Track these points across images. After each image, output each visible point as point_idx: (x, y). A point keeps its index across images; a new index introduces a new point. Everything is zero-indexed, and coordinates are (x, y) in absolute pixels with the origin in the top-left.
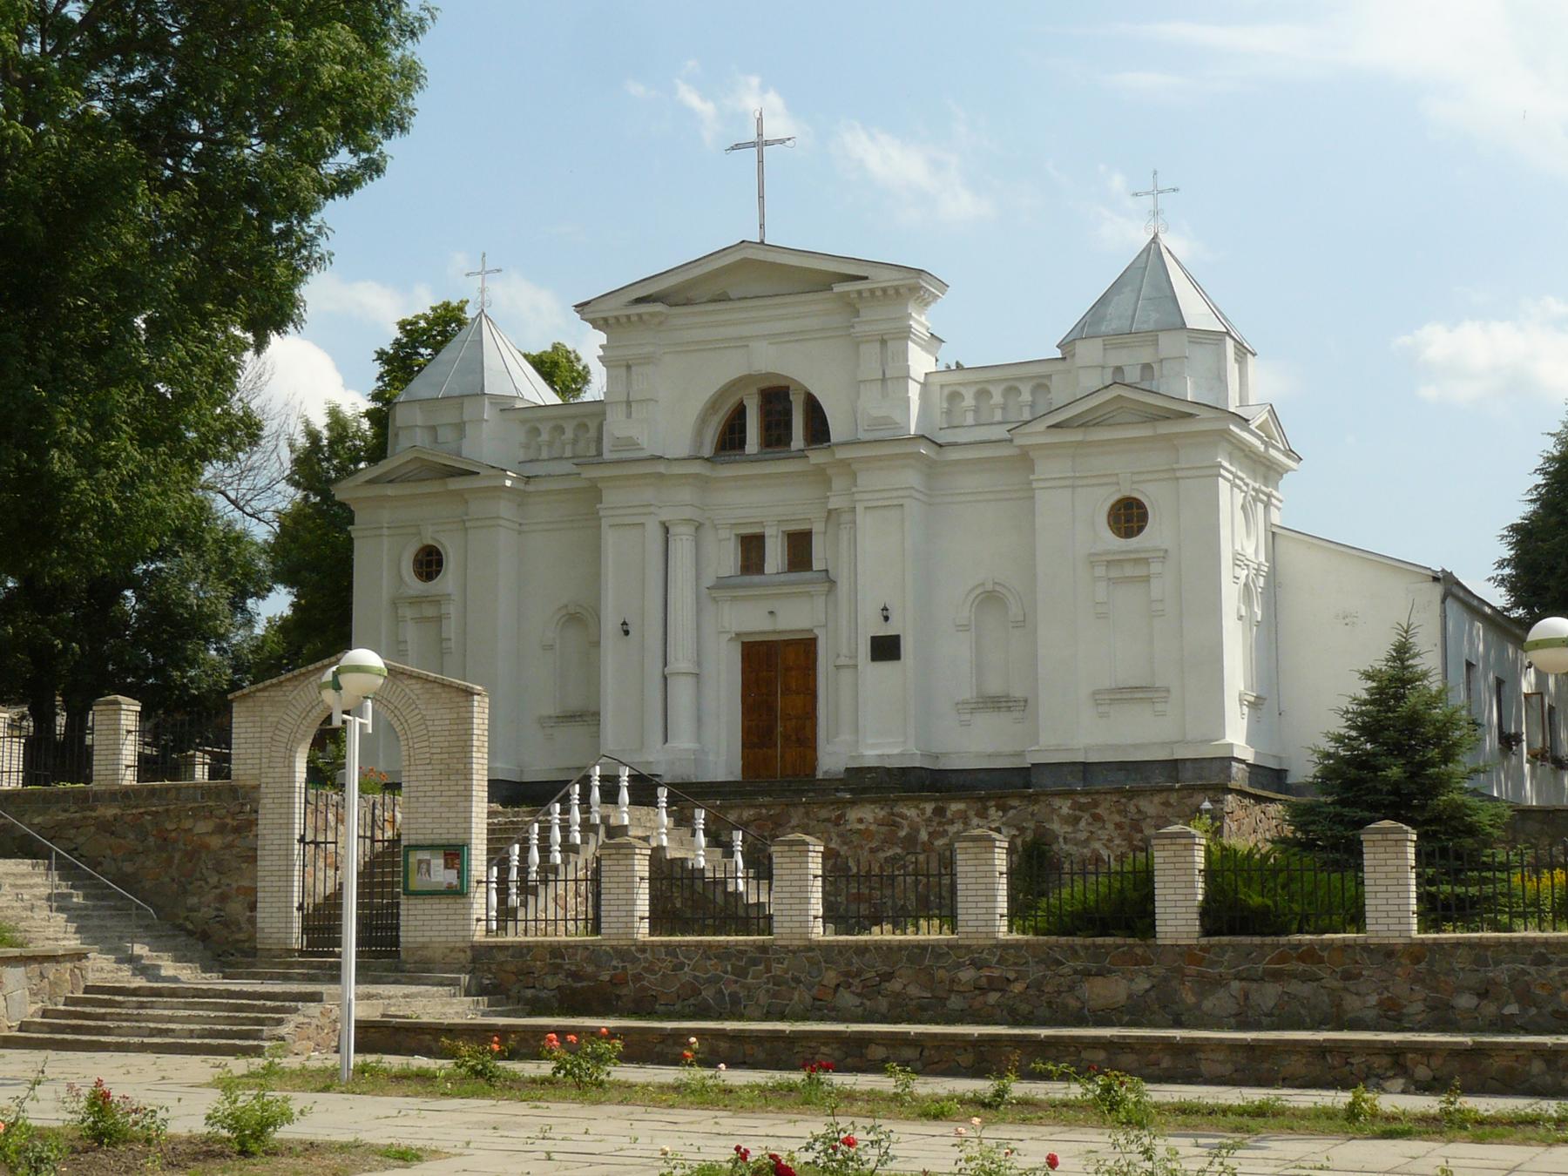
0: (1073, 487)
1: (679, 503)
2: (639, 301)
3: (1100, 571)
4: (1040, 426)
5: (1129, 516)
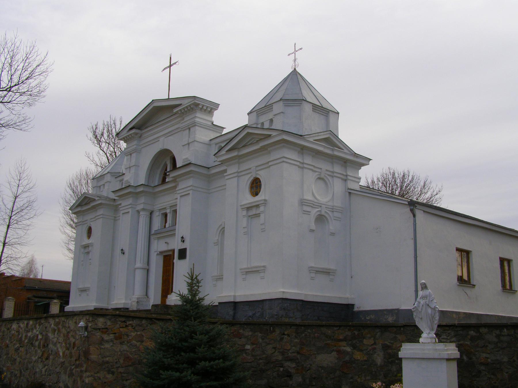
0: (238, 177)
1: (142, 203)
2: (131, 129)
3: (245, 213)
4: (223, 152)
5: (256, 186)
